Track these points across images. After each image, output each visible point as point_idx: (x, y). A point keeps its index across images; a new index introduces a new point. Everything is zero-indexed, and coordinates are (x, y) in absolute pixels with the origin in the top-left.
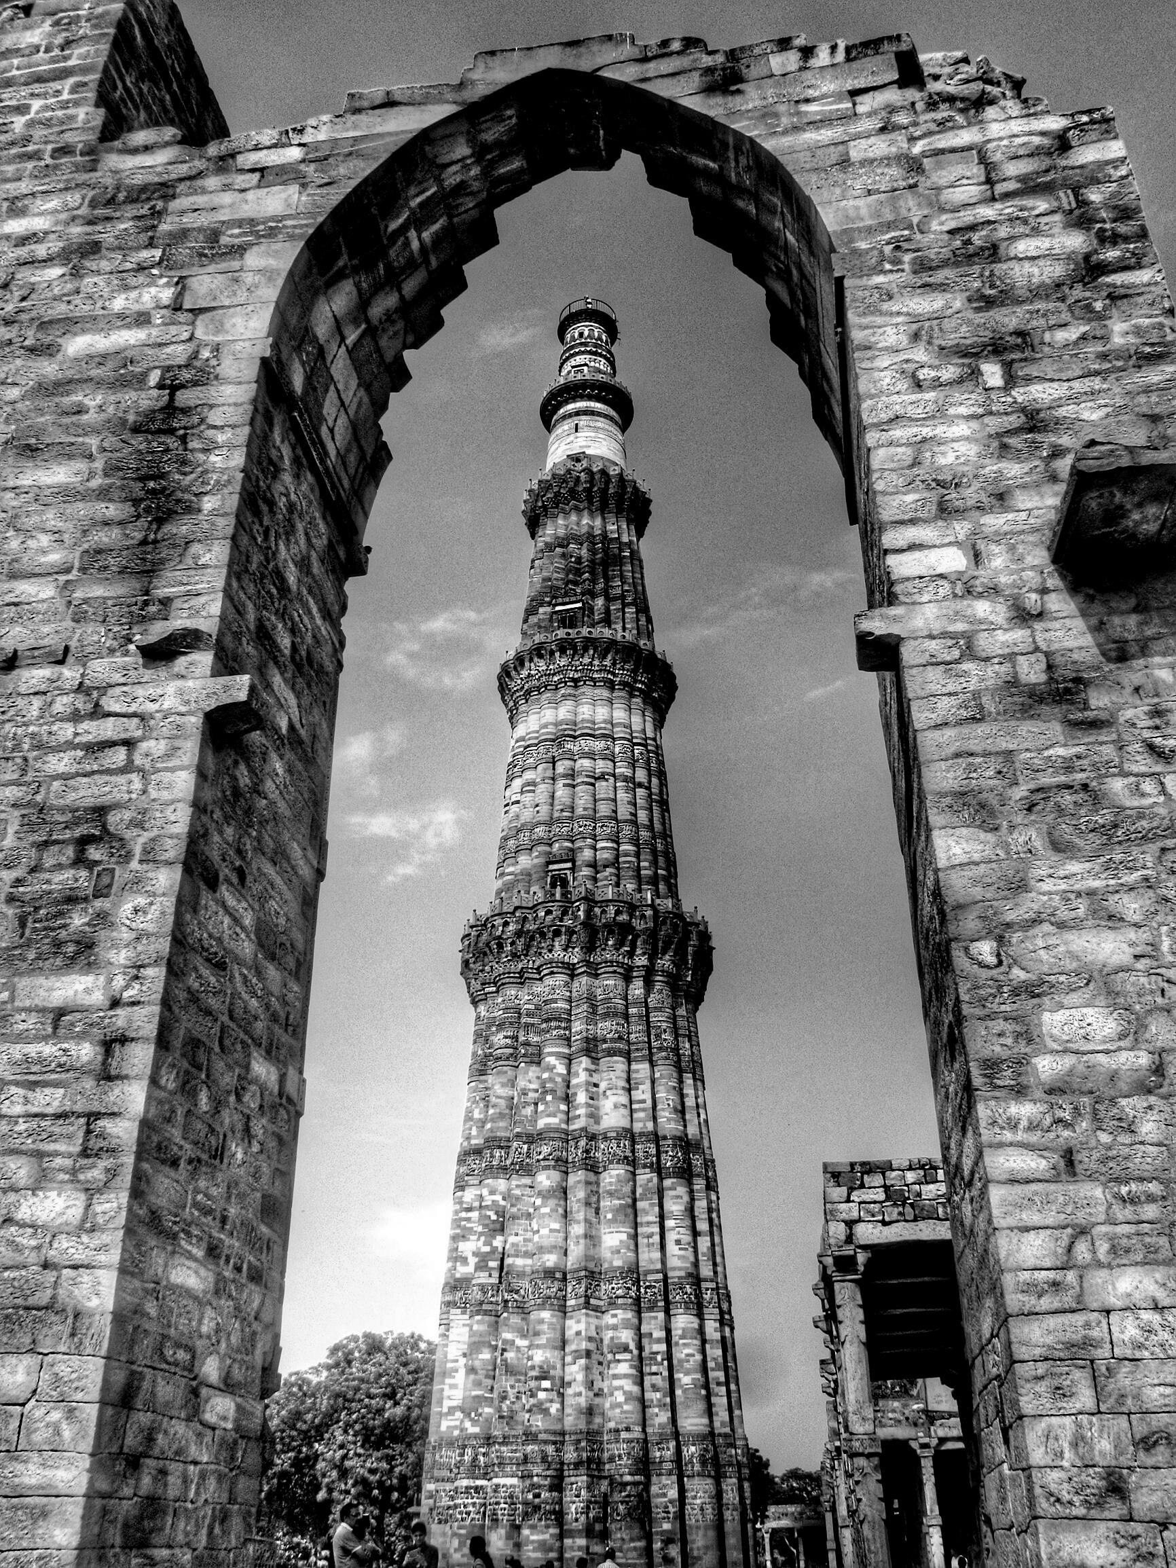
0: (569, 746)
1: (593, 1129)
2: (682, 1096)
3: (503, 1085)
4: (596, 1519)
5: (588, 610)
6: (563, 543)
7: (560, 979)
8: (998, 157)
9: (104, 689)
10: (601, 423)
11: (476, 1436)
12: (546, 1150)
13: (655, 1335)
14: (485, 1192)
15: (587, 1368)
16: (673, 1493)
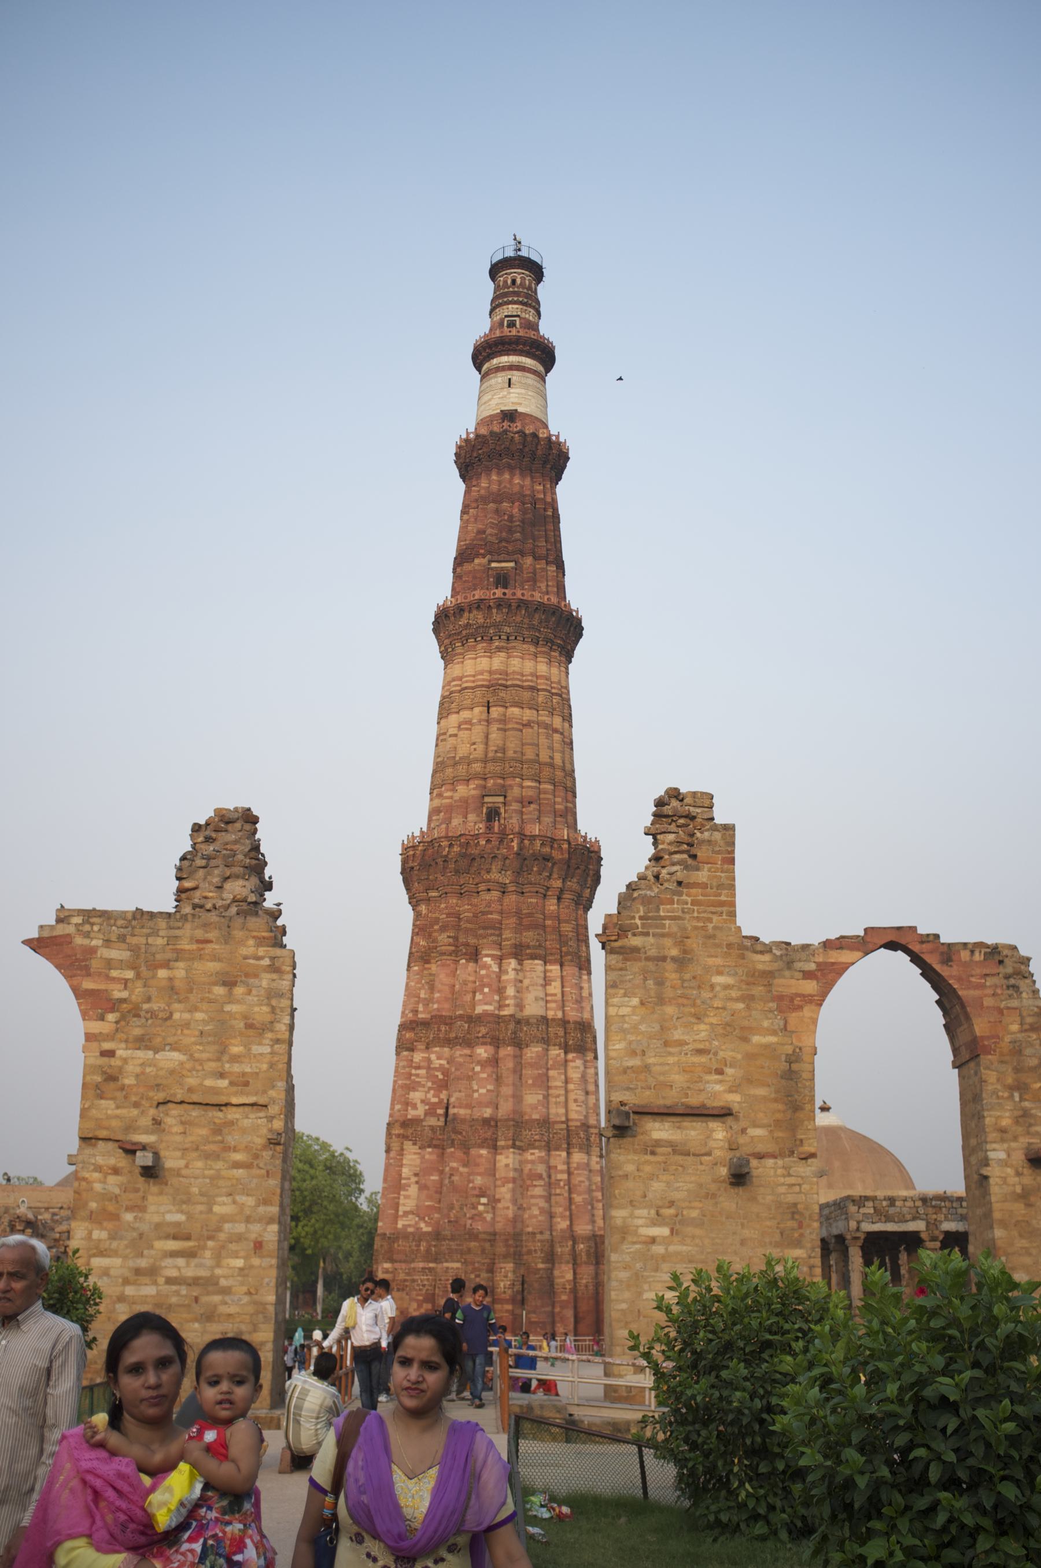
0: (502, 694)
1: (519, 1016)
2: (581, 988)
3: (447, 975)
4: (517, 1292)
5: (518, 567)
6: (498, 498)
7: (495, 894)
8: (1025, 1014)
9: (790, 1168)
10: (531, 379)
11: (428, 1233)
12: (483, 1030)
13: (559, 1168)
14: (433, 1057)
16: (570, 1276)
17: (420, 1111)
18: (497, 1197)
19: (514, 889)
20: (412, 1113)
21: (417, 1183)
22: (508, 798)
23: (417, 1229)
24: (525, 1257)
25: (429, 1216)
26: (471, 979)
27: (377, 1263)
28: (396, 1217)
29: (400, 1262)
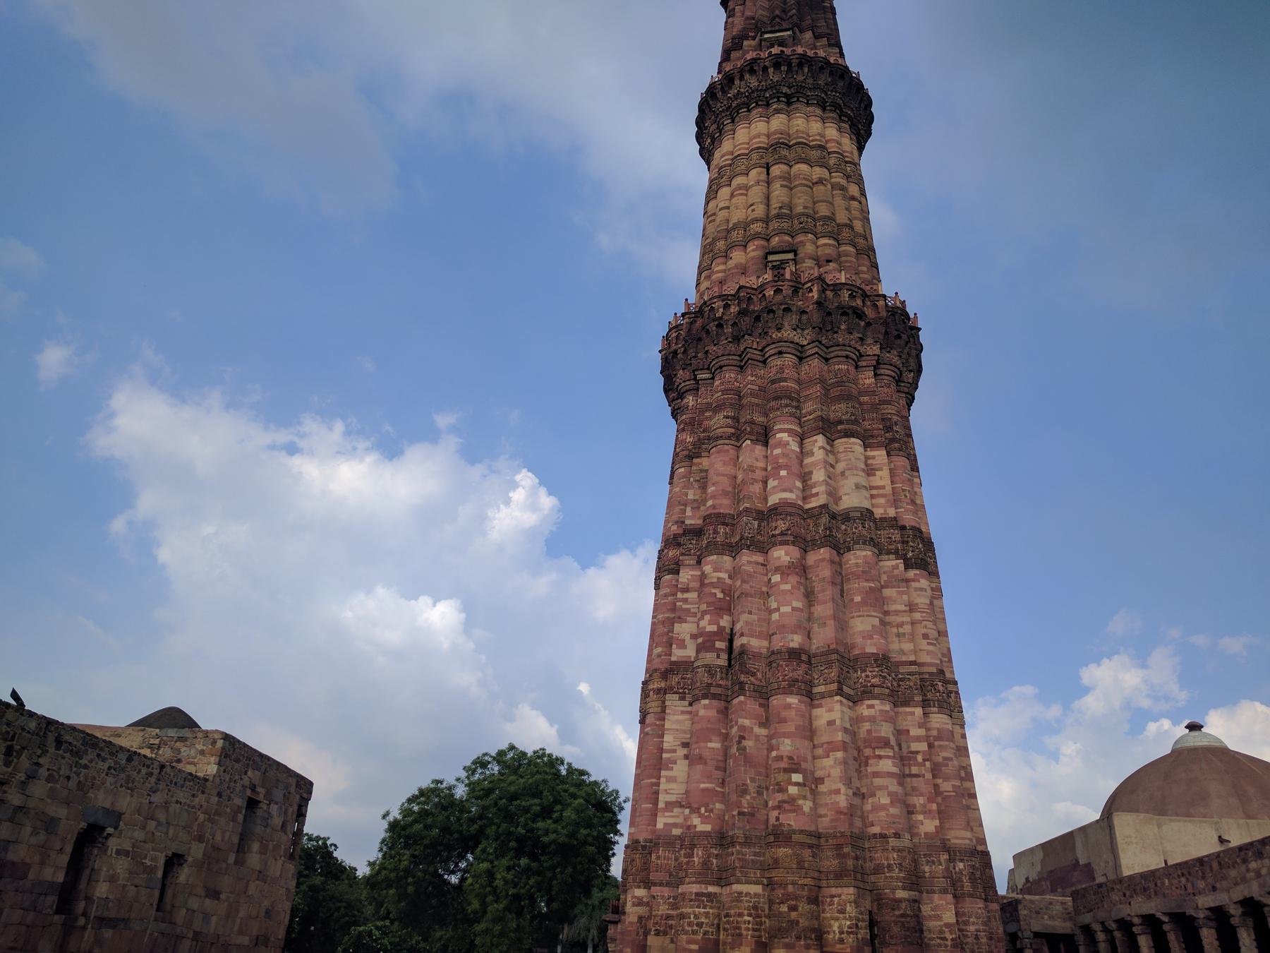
1: (834, 508)
3: (725, 463)
11: (706, 835)
12: (782, 525)
13: (912, 733)
14: (708, 569)
15: (845, 763)
17: (690, 652)
18: (818, 774)
19: (813, 351)
20: (678, 654)
21: (686, 757)
22: (801, 255)
23: (689, 827)
24: (873, 878)
25: (706, 806)
26: (761, 464)
27: (625, 891)
28: (654, 815)
29: (661, 885)
